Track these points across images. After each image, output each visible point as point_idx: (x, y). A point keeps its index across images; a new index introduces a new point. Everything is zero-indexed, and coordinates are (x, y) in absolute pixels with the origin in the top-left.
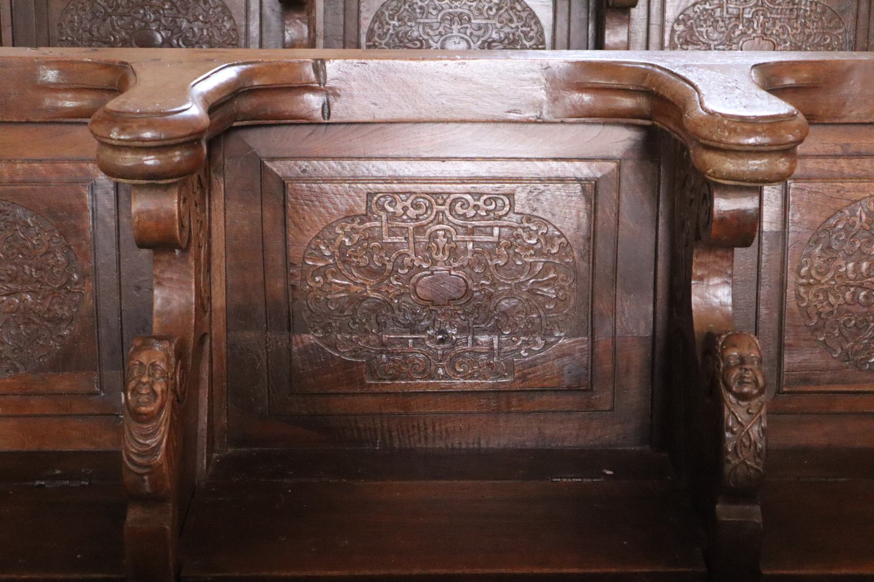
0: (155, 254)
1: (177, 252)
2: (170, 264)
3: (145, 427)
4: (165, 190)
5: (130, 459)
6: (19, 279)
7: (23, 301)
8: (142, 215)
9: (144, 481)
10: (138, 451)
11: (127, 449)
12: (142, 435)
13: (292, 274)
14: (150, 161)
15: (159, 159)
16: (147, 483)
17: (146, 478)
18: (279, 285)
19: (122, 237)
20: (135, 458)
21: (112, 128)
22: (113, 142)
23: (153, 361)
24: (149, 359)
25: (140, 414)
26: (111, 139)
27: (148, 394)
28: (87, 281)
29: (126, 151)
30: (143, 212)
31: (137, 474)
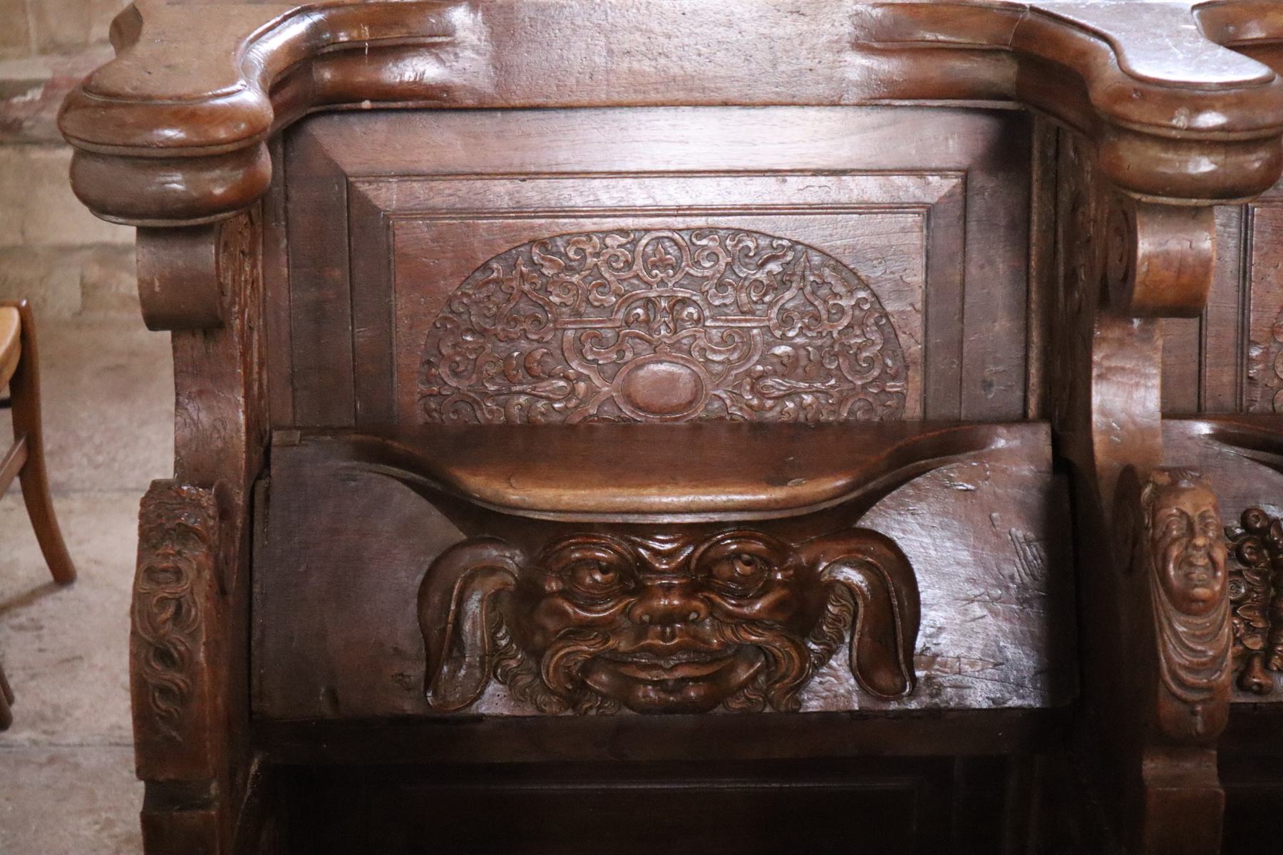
0: (1145, 323)
1: (1136, 322)
2: (1121, 343)
3: (1199, 621)
4: (1194, 217)
5: (1176, 677)
6: (800, 371)
7: (801, 407)
8: (1155, 260)
9: (1194, 713)
10: (1191, 662)
11: (1169, 659)
12: (1194, 636)
13: (1250, 359)
14: (1203, 165)
15: (1216, 163)
16: (1199, 718)
17: (1199, 708)
18: (1227, 377)
19: (967, 299)
20: (1183, 674)
21: (1175, 109)
22: (1174, 133)
23: (1204, 509)
24: (1196, 507)
25: (1196, 600)
26: (1174, 128)
27: (1205, 567)
28: (910, 373)
29: (1190, 149)
30: (1157, 256)
31: (1185, 702)
